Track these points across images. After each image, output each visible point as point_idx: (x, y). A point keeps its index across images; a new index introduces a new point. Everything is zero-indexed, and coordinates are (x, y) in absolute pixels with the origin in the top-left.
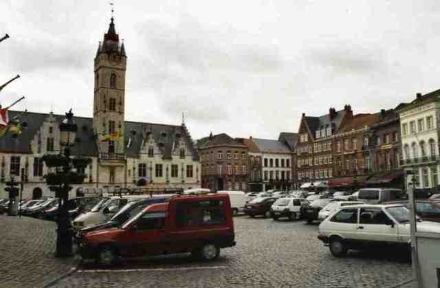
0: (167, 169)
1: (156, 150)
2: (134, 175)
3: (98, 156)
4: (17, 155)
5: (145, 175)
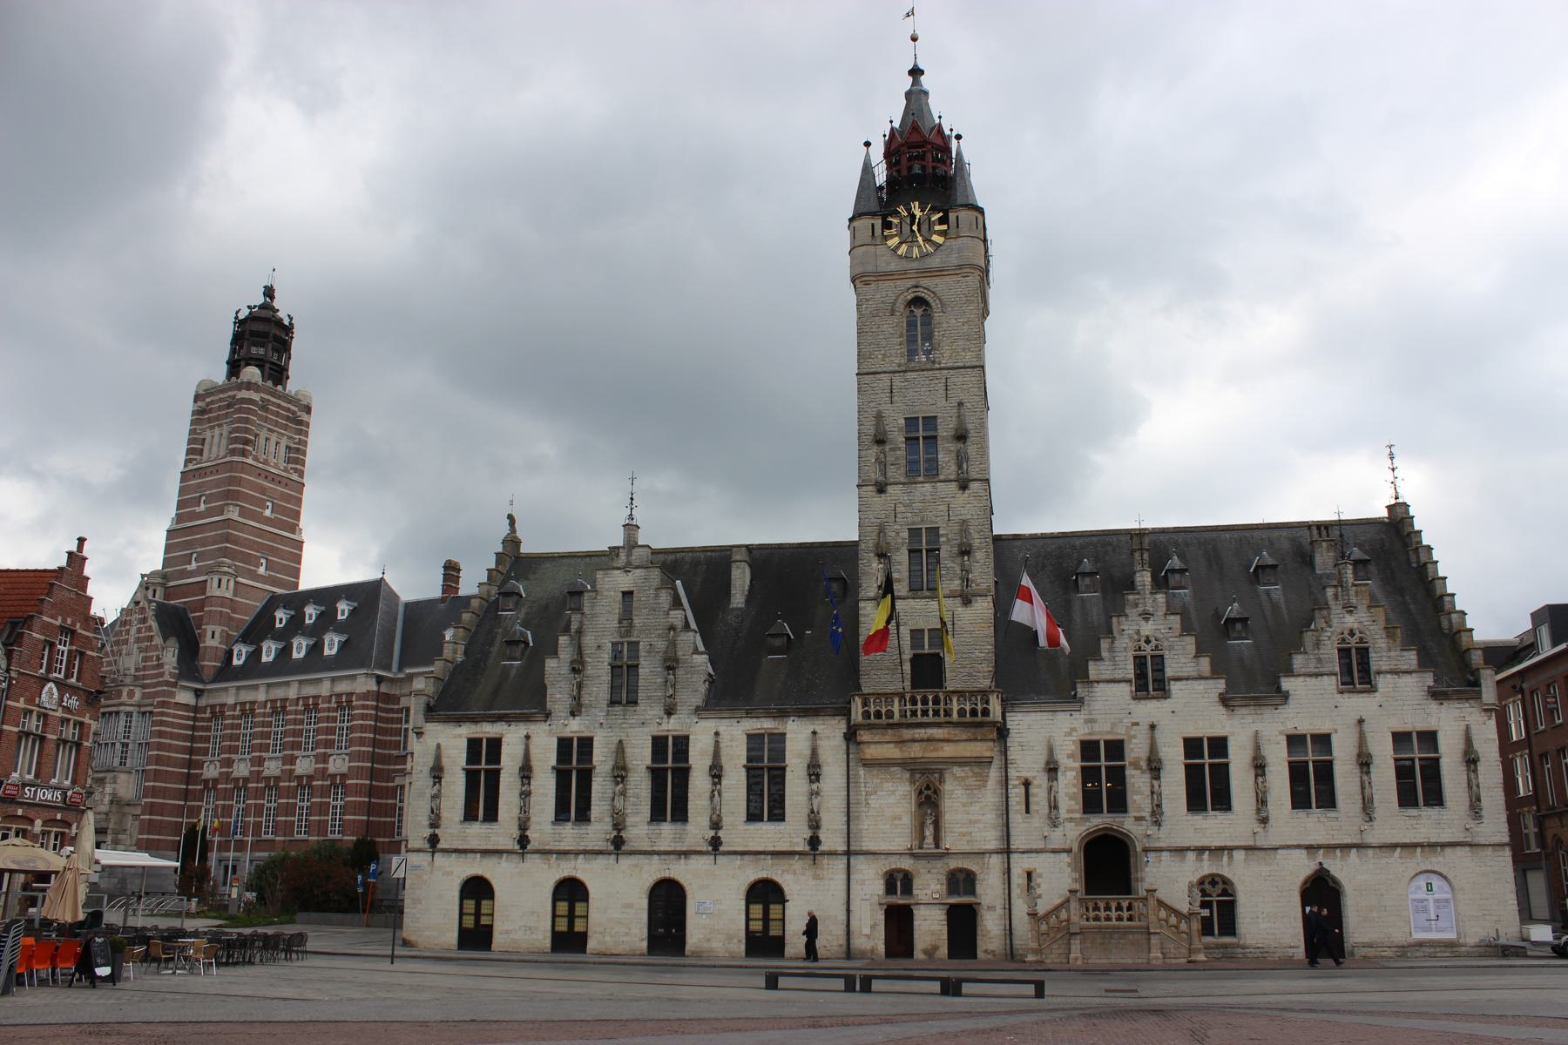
0: (1259, 767)
1: (1181, 658)
2: (1053, 806)
3: (846, 713)
4: (488, 730)
5: (1119, 803)
